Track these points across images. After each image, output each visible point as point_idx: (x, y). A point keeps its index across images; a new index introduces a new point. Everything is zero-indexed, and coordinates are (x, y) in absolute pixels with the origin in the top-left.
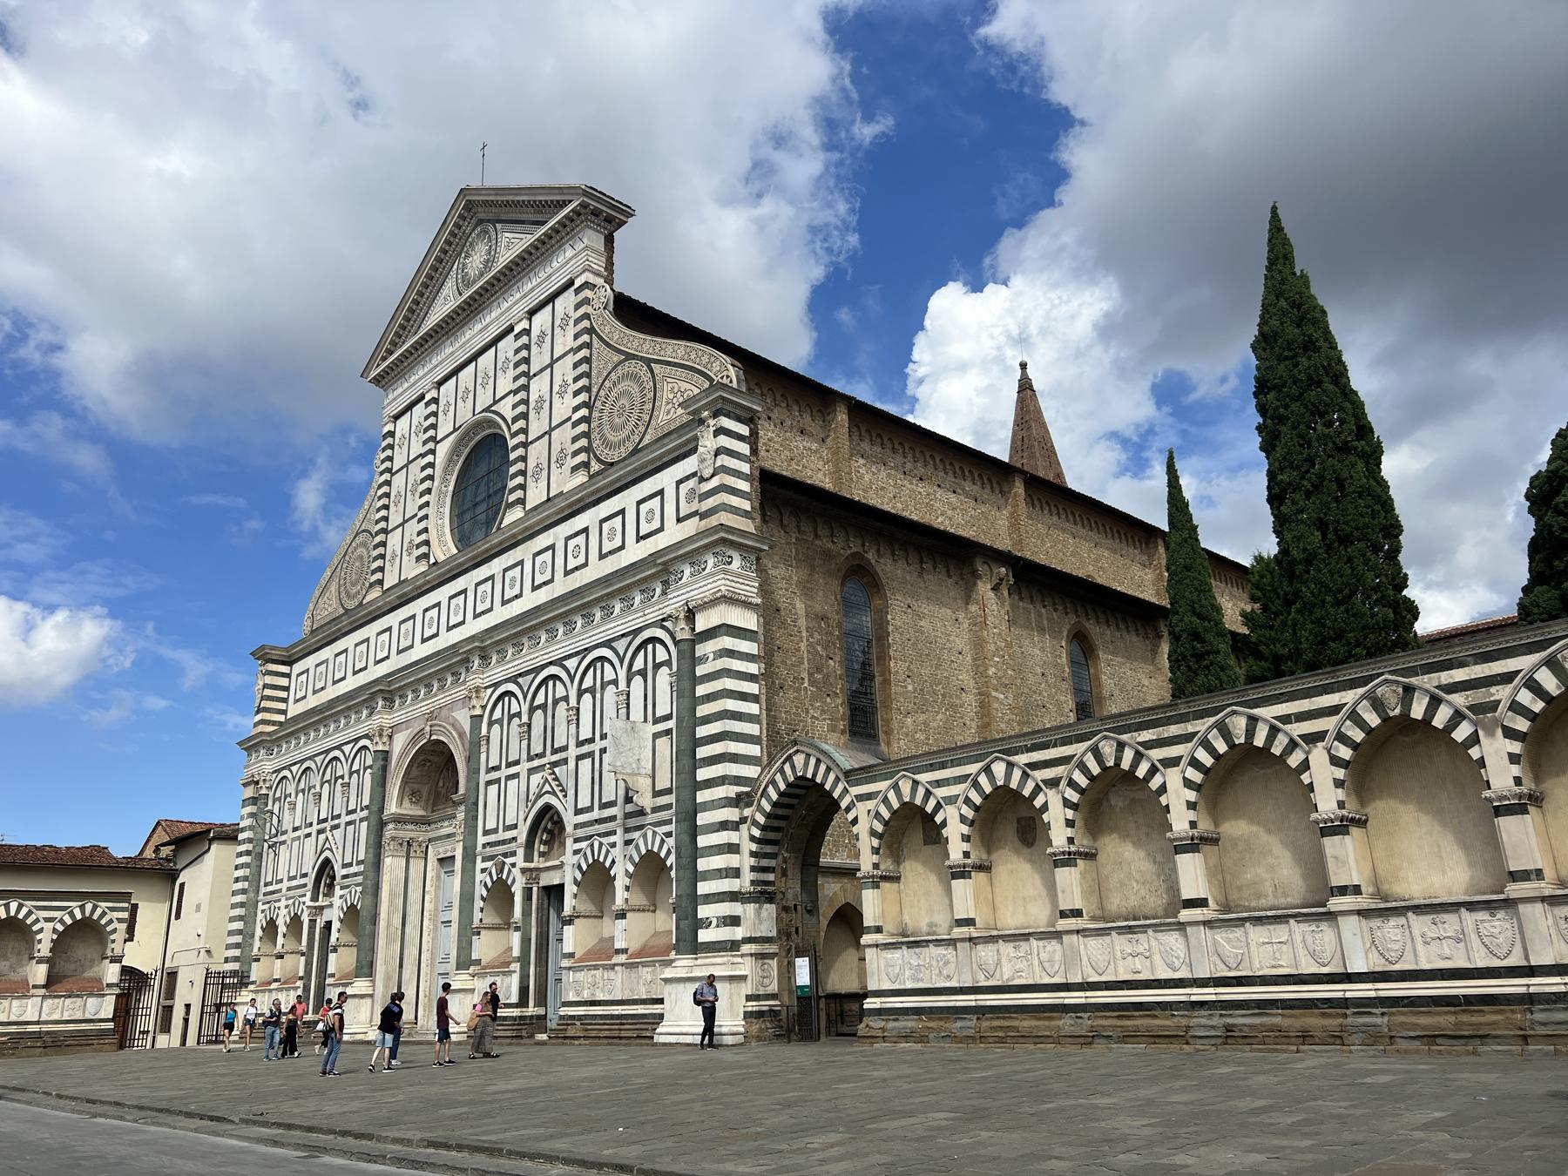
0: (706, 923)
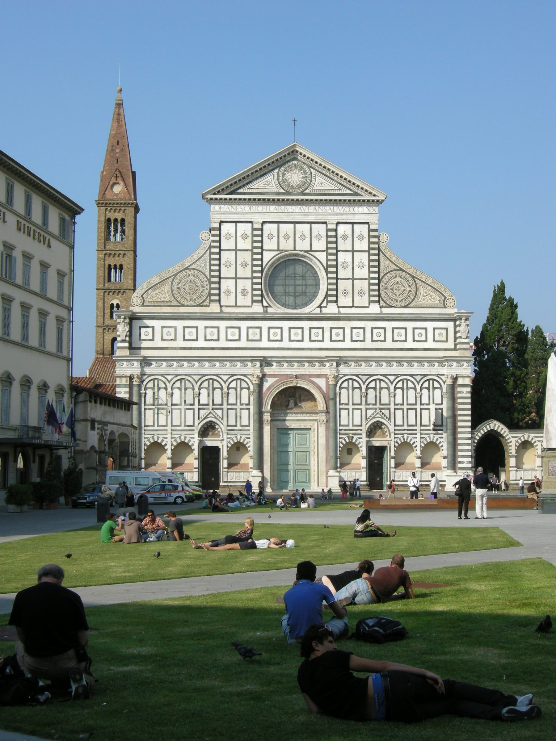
0: (463, 462)
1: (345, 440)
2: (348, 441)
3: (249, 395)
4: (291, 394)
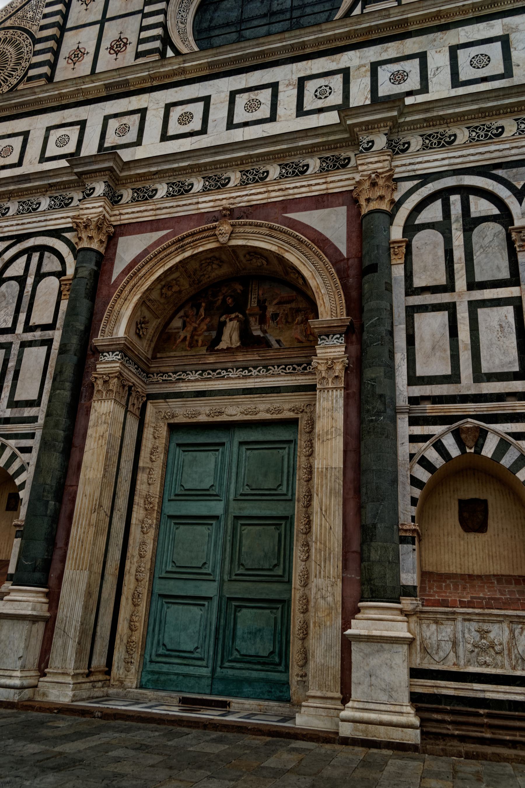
1: (439, 447)
2: (454, 452)
3: (60, 293)
4: (229, 301)
